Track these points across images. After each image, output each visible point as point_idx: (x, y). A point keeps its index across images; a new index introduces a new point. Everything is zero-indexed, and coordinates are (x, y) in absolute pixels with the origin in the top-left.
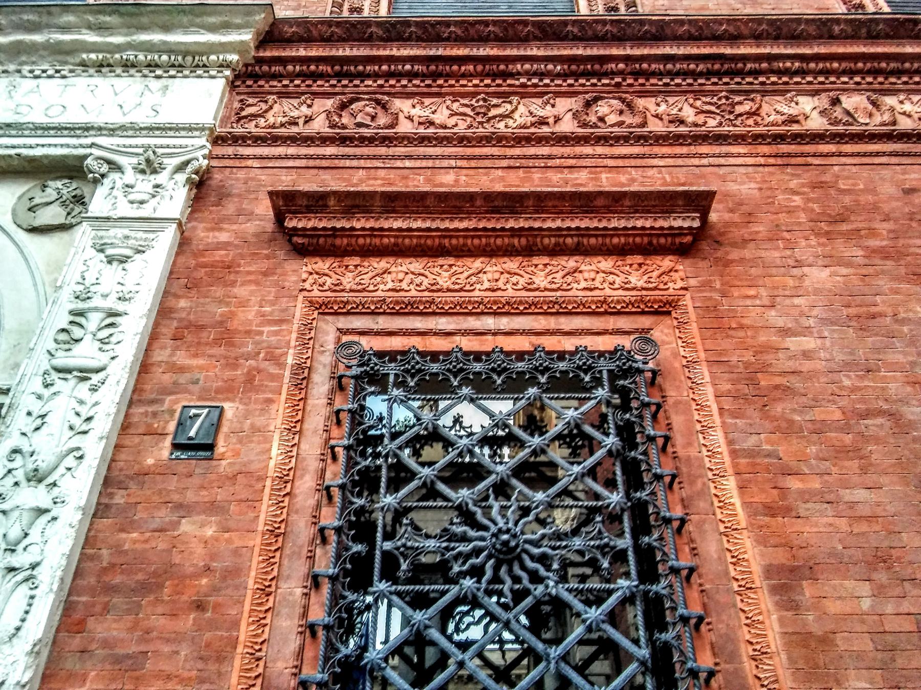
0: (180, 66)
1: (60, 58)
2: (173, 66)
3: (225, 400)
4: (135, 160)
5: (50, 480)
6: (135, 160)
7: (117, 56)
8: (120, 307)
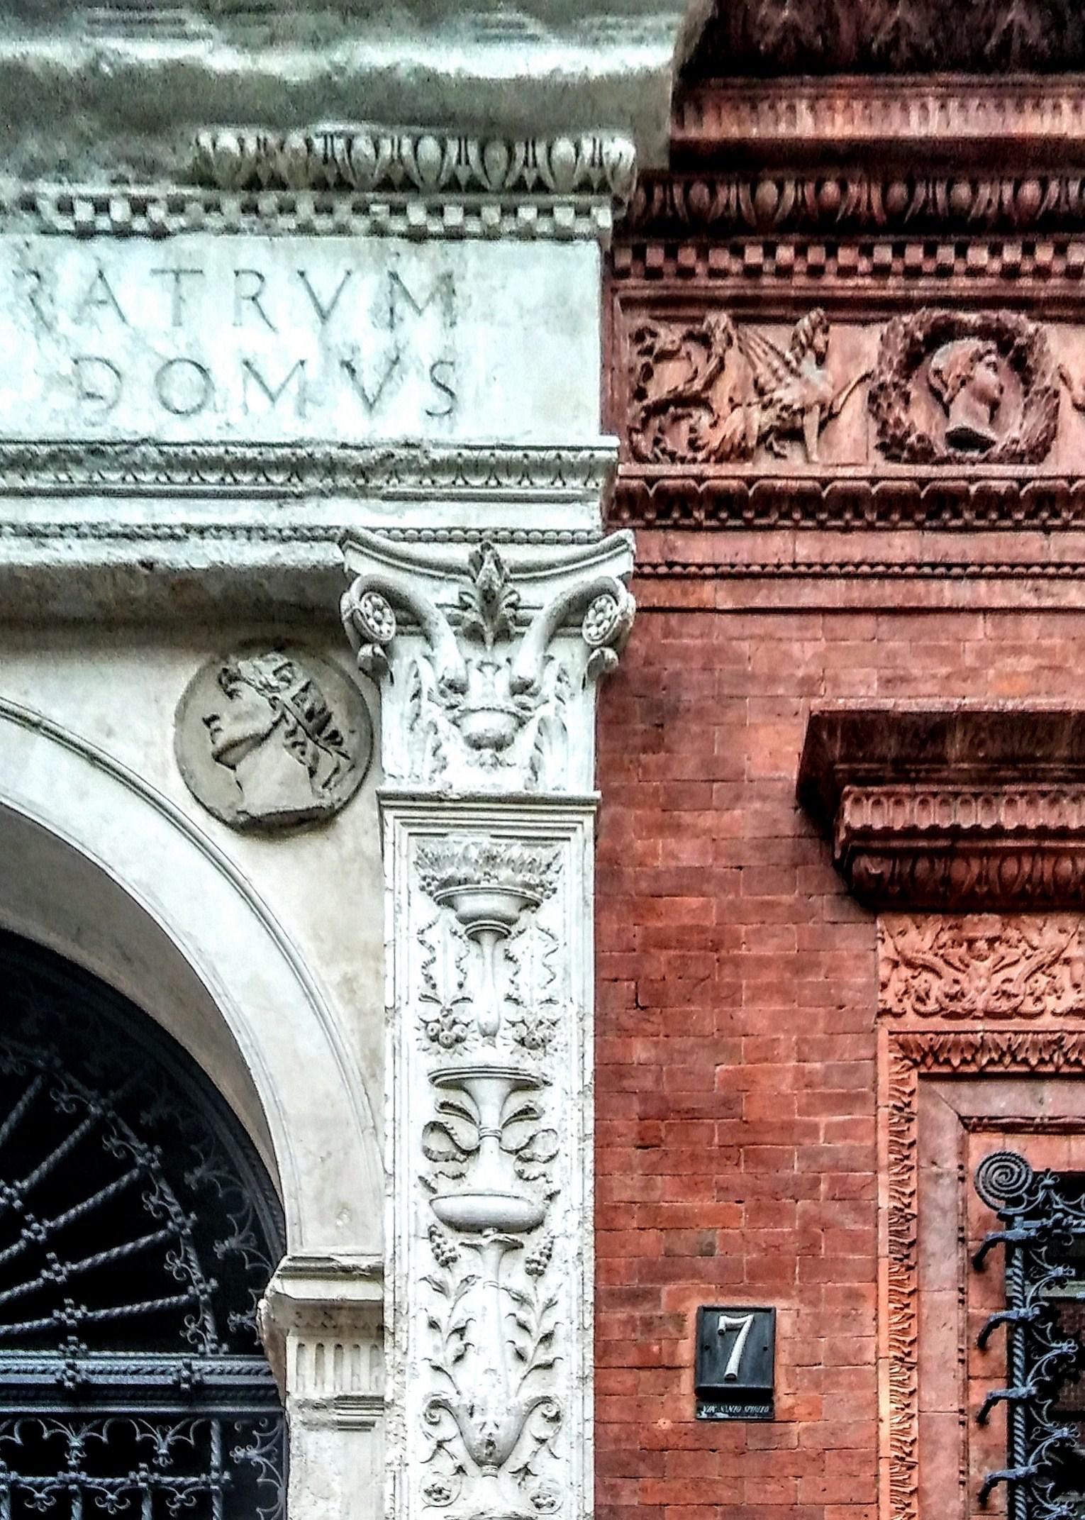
3: (771, 1294)
4: (450, 593)
5: (514, 1463)
6: (450, 593)
8: (531, 1065)
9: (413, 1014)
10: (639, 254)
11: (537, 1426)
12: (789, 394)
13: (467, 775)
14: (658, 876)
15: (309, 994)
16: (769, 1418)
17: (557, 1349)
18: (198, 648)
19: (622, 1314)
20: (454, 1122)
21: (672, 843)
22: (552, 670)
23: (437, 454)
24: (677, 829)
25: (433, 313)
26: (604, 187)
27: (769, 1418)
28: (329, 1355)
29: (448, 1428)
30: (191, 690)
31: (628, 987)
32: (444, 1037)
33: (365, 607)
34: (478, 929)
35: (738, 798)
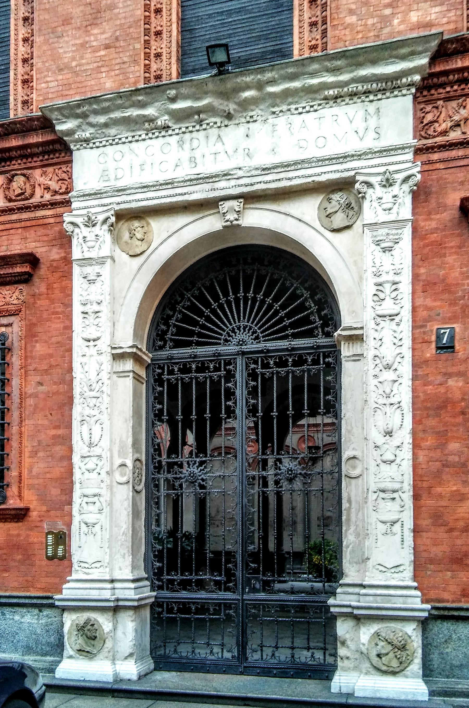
0: (384, 90)
1: (311, 96)
2: (380, 90)
3: (455, 323)
4: (379, 178)
5: (393, 368)
6: (379, 178)
7: (346, 89)
8: (397, 279)
9: (371, 270)
10: (421, 93)
11: (398, 359)
12: (456, 118)
13: (383, 217)
14: (426, 230)
15: (346, 265)
16: (453, 352)
17: (403, 341)
18: (322, 193)
19: (418, 331)
20: (379, 293)
21: (430, 223)
22: (402, 191)
23: (376, 150)
24: (431, 219)
25: (375, 118)
26: (413, 85)
27: (453, 352)
28: (351, 344)
29: (378, 361)
30: (321, 203)
31: (419, 257)
32: (377, 275)
33: (360, 187)
34: (384, 250)
35: (445, 210)
